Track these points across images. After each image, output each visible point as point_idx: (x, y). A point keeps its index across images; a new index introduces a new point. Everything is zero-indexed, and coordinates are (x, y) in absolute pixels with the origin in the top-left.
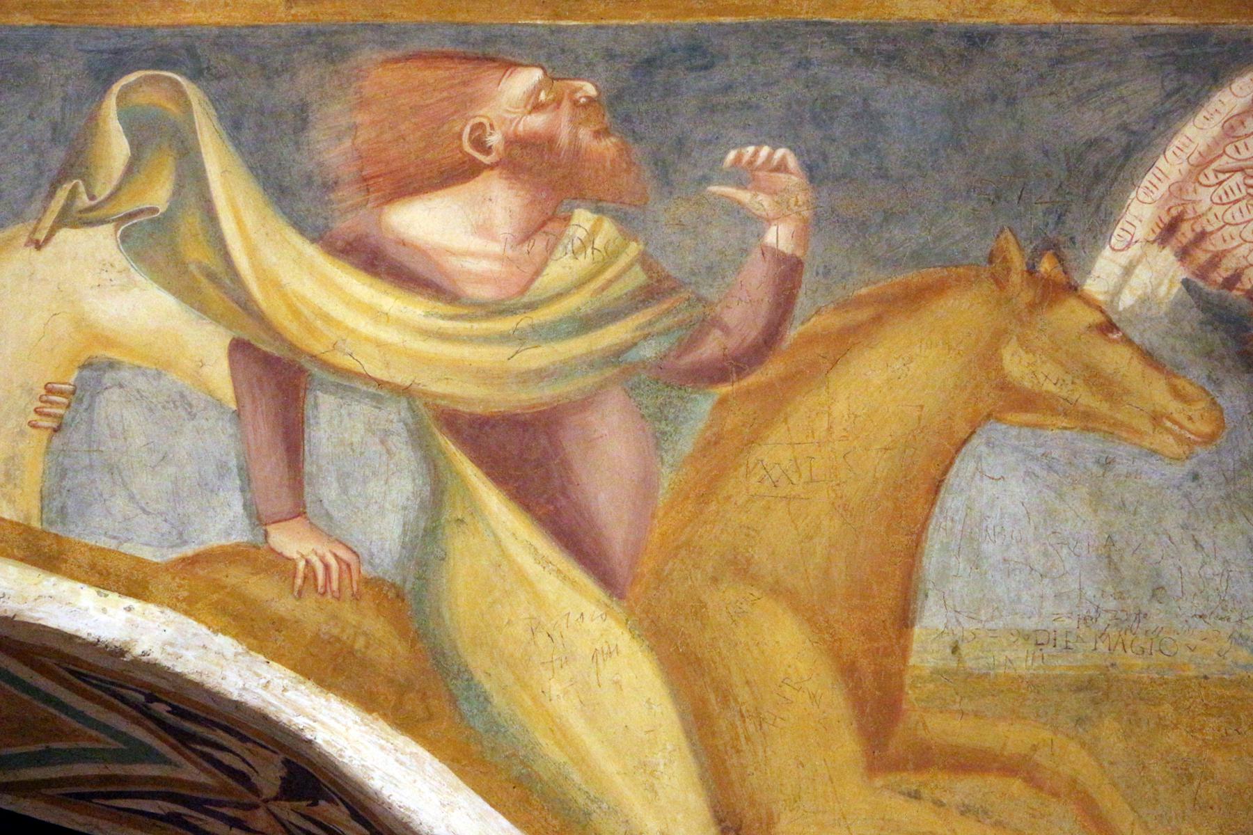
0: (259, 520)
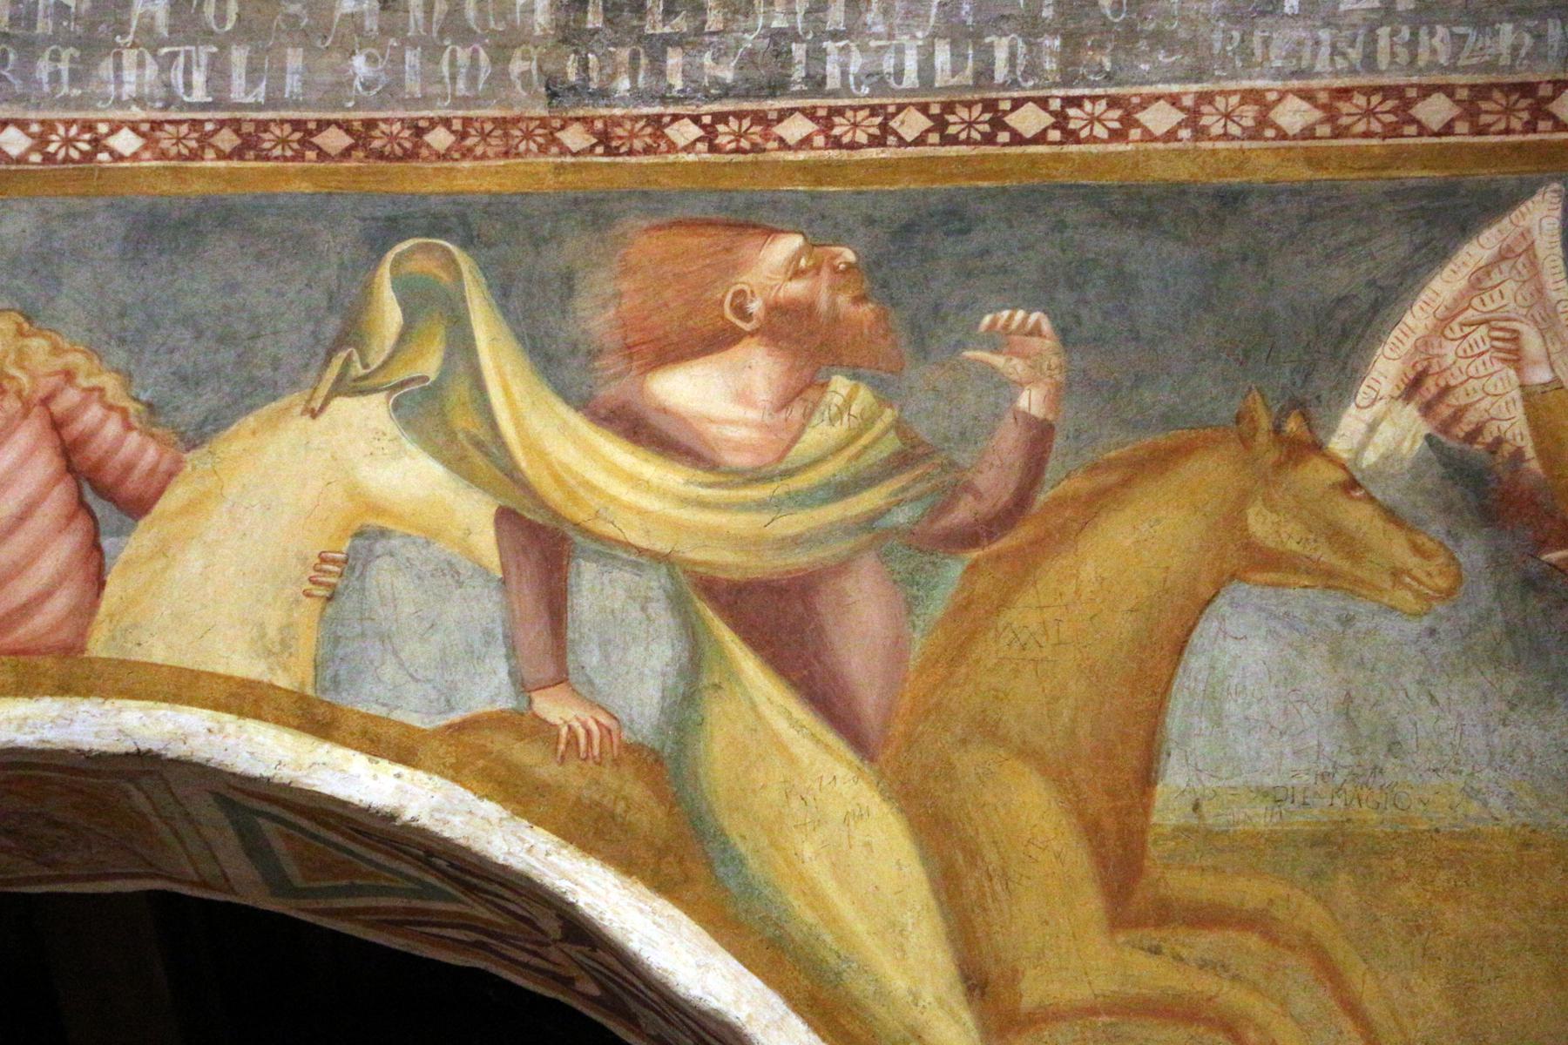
0: (523, 686)
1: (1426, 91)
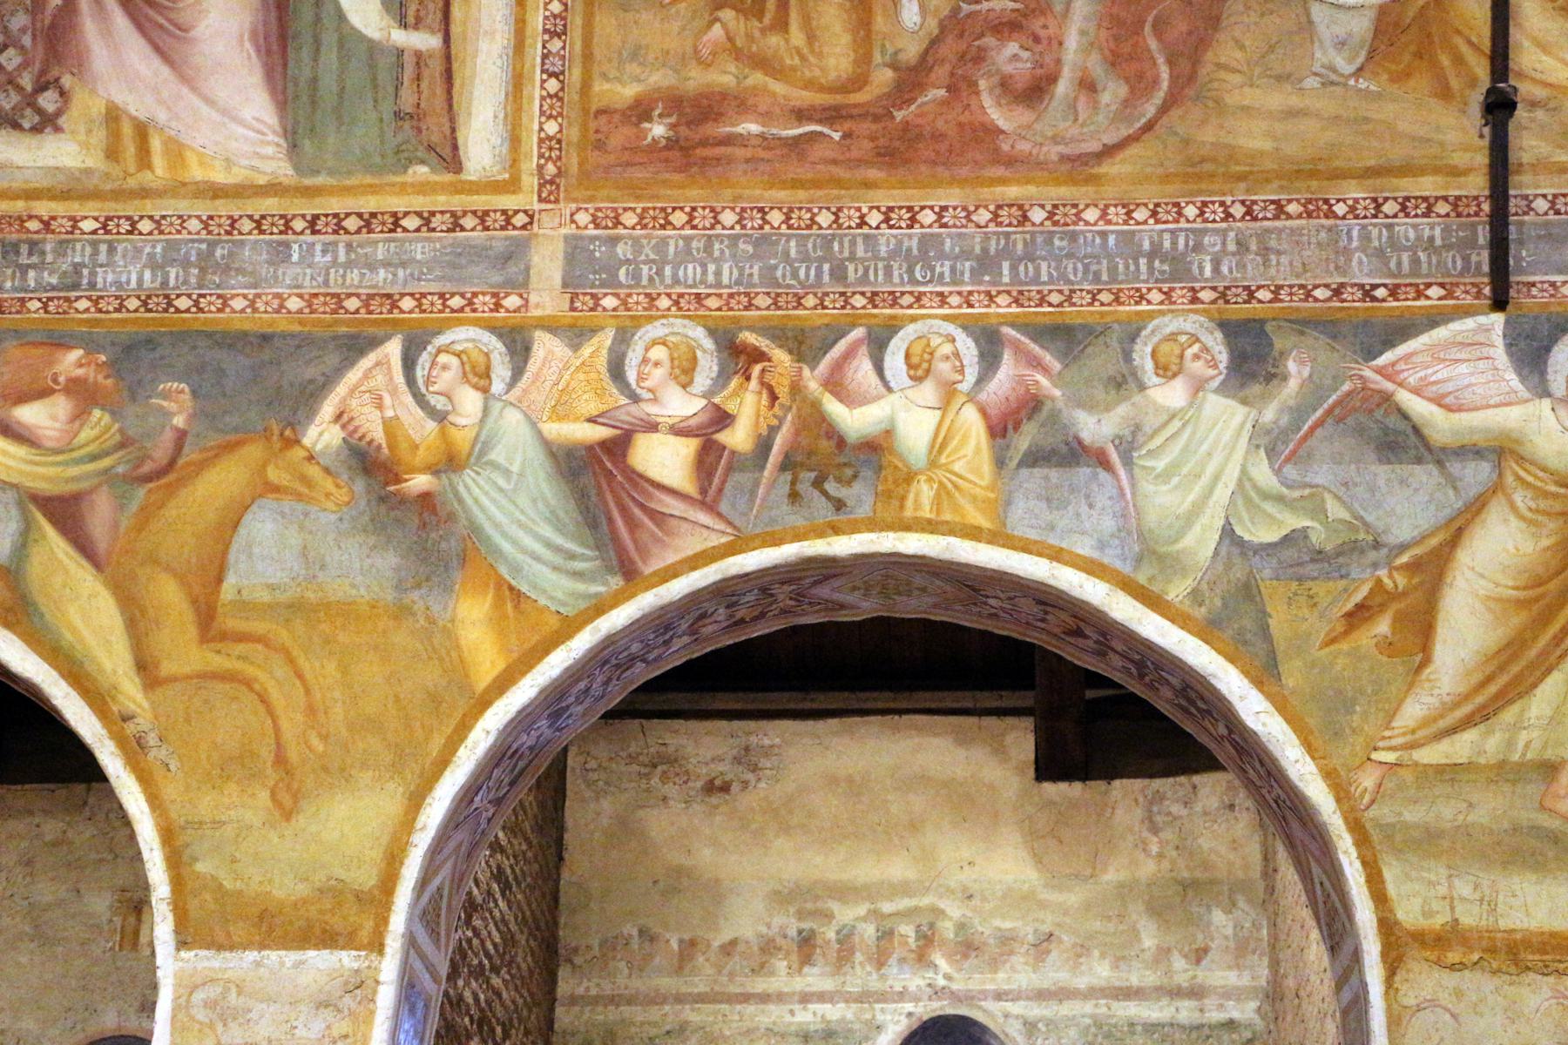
1: (349, 295)
